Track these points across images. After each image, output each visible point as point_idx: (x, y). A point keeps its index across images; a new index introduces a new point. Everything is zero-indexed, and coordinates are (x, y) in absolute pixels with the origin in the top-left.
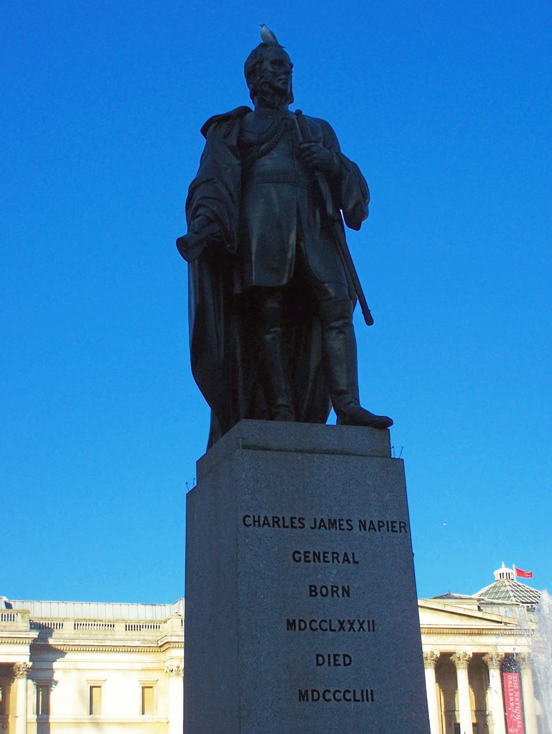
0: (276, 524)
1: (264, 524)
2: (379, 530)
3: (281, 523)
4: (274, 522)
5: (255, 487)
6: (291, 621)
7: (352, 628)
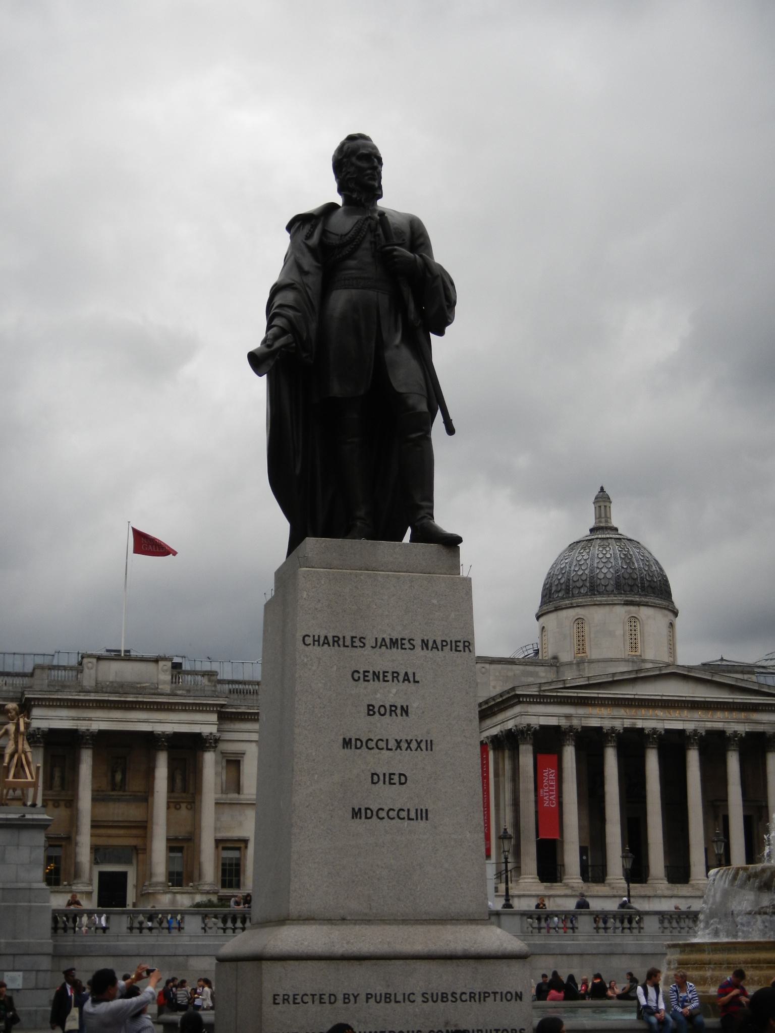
1: (324, 643)
3: (341, 642)
4: (334, 641)
7: (409, 747)
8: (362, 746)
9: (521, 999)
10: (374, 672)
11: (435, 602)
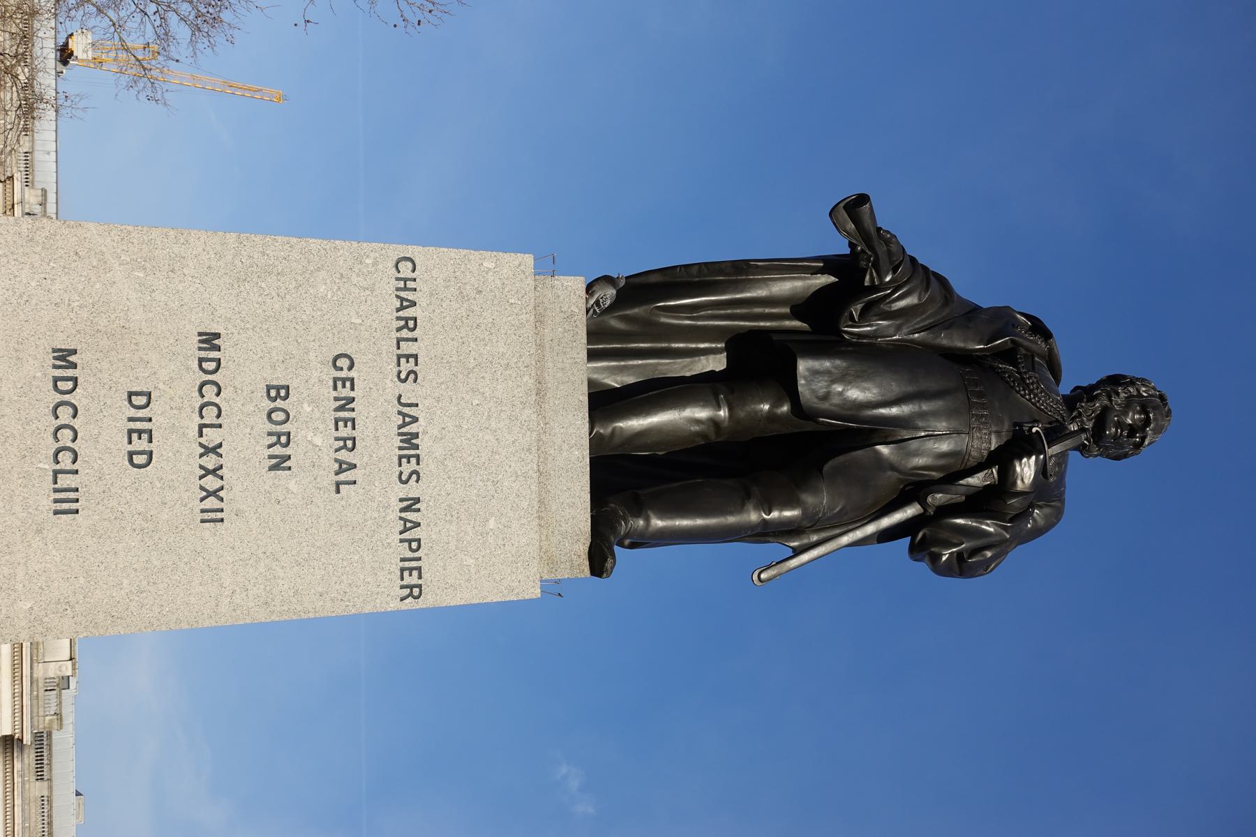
0: (403, 323)
1: (402, 299)
2: (402, 541)
3: (405, 333)
4: (407, 319)
5: (468, 287)
6: (216, 342)
7: (208, 472)
8: (206, 372)
10: (353, 399)
11: (492, 524)
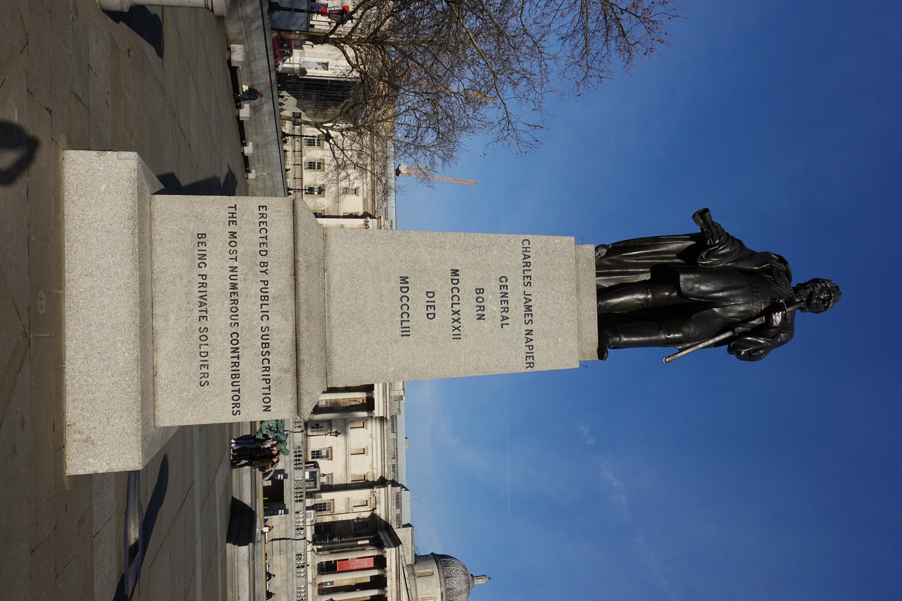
3: (526, 268)
9: (265, 410)
11: (560, 340)
